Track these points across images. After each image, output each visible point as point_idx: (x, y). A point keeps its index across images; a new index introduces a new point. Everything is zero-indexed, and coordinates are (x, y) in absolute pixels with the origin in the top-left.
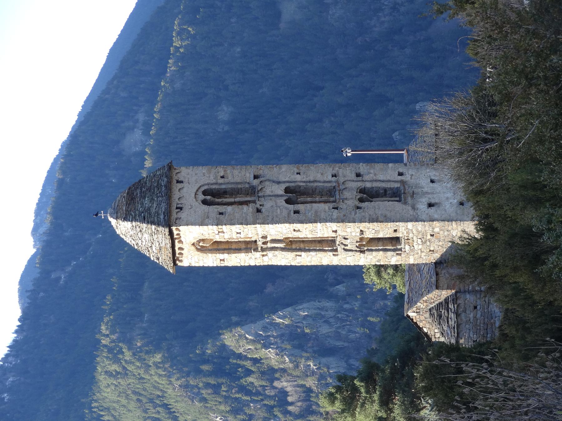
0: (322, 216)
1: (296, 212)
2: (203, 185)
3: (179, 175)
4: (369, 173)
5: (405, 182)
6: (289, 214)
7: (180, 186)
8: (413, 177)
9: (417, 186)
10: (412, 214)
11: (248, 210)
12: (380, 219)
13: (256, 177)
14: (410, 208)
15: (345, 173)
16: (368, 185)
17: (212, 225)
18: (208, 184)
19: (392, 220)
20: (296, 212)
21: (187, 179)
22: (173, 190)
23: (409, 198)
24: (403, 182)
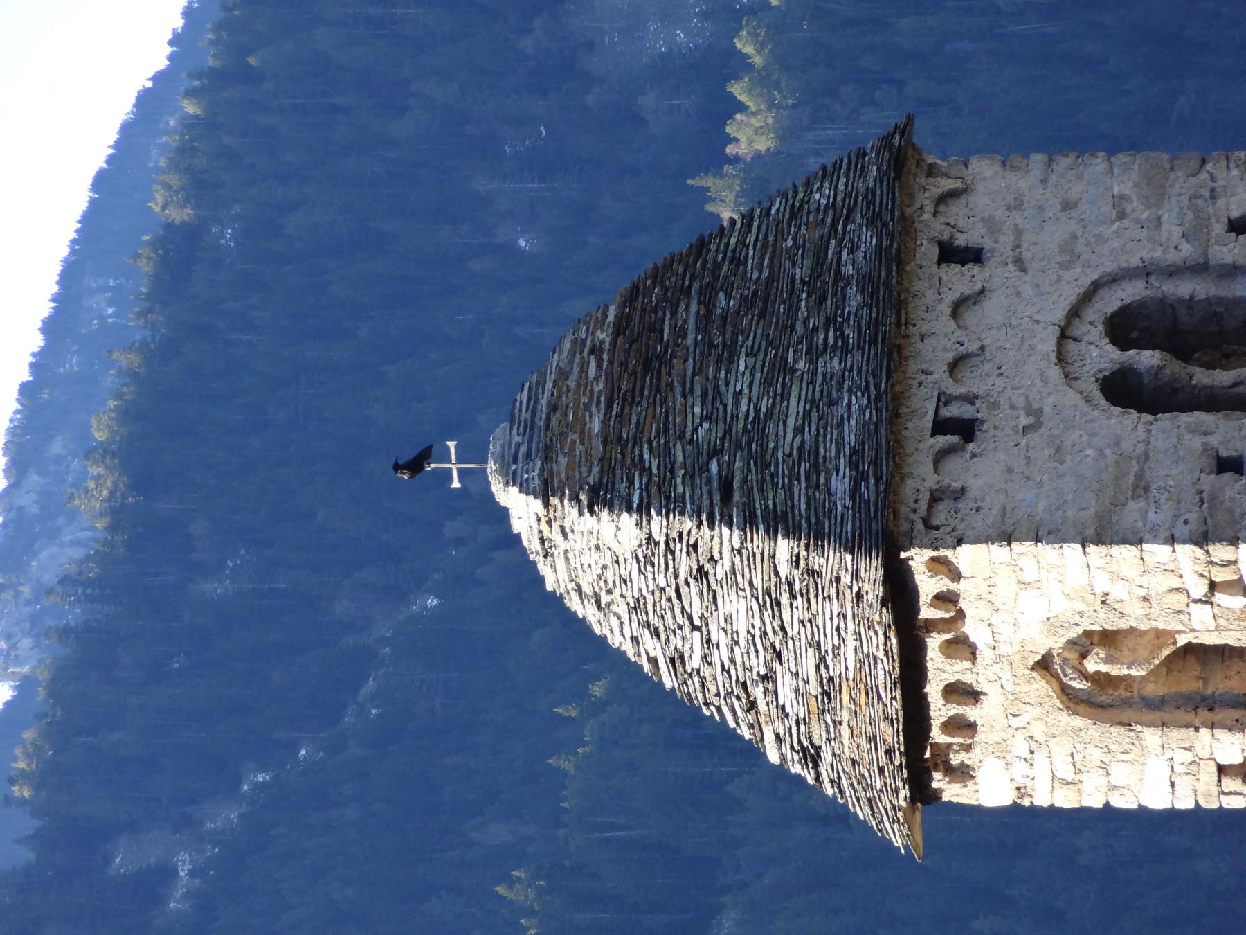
2: (1113, 280)
3: (956, 211)
17: (1172, 540)
18: (1146, 272)
21: (1007, 239)
22: (916, 309)
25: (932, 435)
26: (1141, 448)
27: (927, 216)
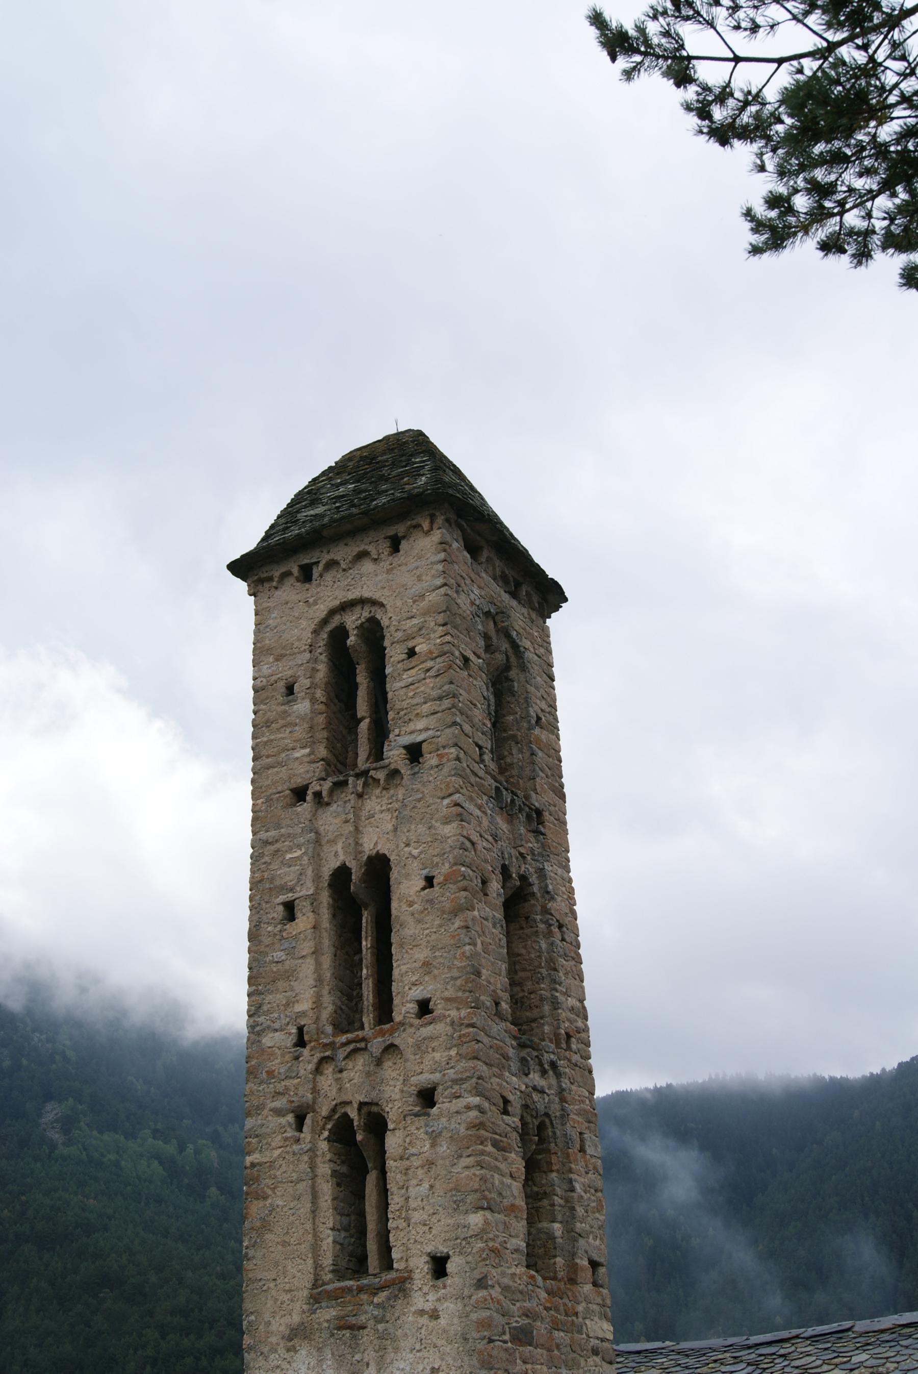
0: (270, 997)
1: (290, 910)
4: (434, 1138)
6: (284, 889)
7: (385, 547)
8: (424, 1320)
10: (274, 1327)
11: (303, 763)
13: (414, 752)
14: (296, 1319)
15: (435, 1044)
16: (392, 1142)
17: (255, 679)
19: (251, 1253)
20: (290, 910)
23: (334, 1313)
24: (402, 1286)
25: (299, 566)
26: (296, 651)
27: (409, 523)
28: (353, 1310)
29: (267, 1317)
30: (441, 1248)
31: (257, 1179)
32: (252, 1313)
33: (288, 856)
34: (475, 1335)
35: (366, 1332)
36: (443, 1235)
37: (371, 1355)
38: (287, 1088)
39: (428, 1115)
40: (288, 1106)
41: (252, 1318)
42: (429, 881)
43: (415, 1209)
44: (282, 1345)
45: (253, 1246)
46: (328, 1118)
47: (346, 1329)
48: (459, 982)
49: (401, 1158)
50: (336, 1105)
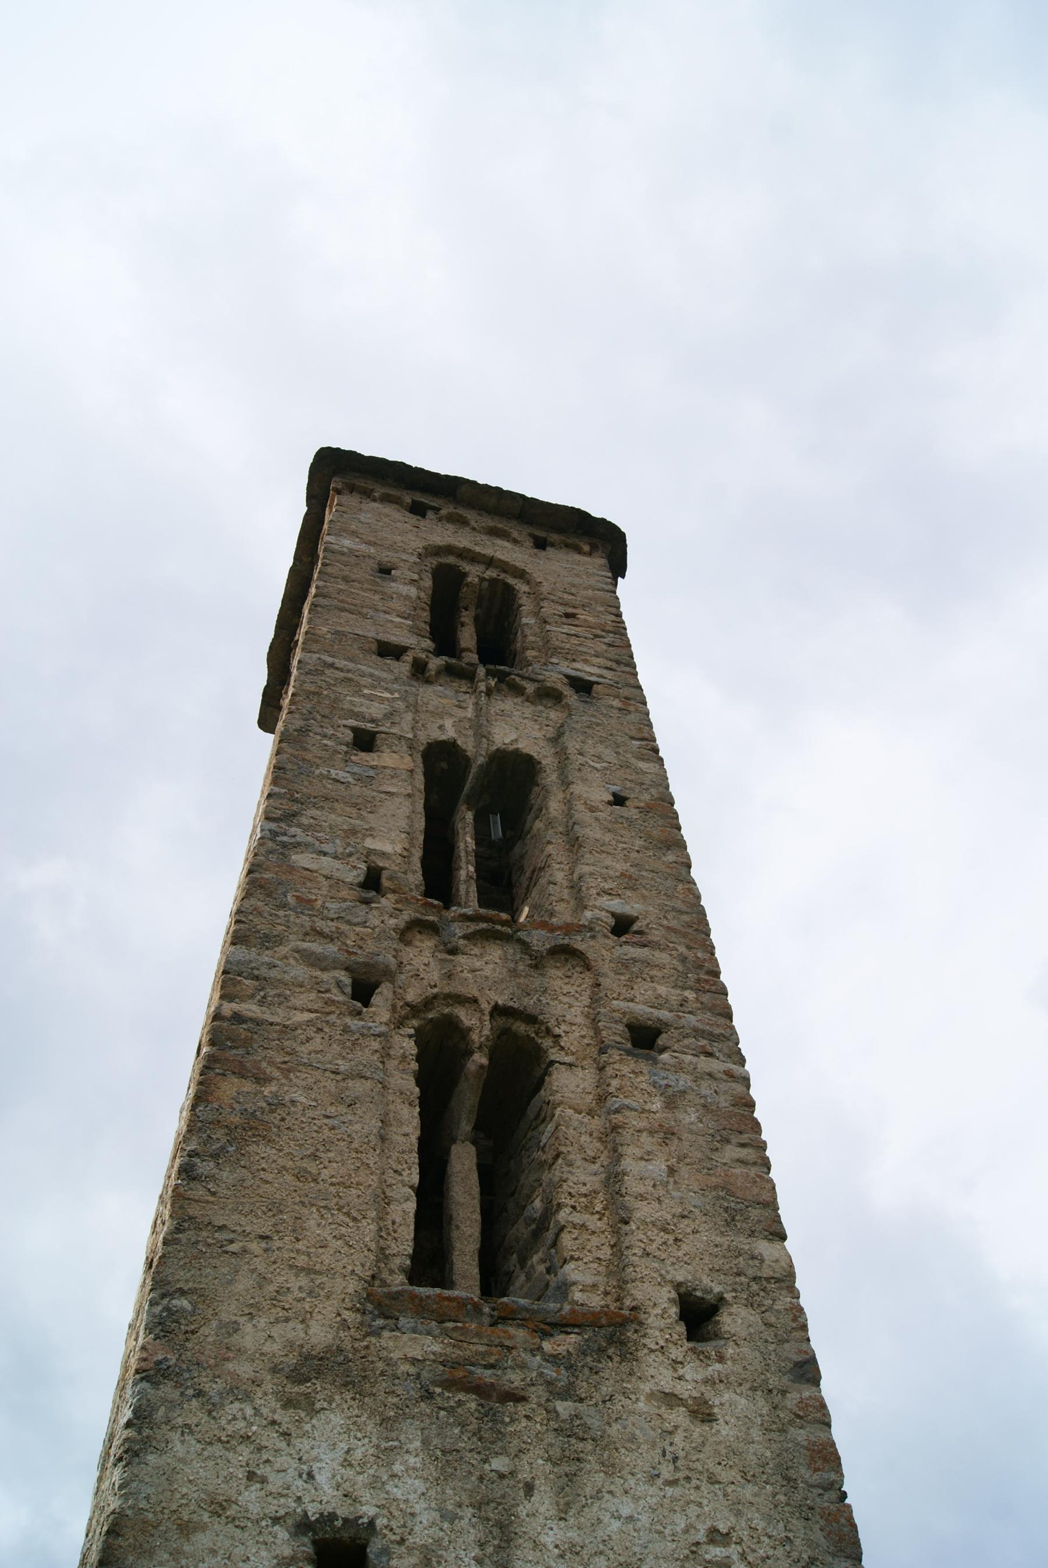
5: (627, 1353)
8: (678, 1416)
9: (577, 1448)
10: (249, 1337)
12: (229, 1088)
14: (320, 1334)
15: (654, 972)
16: (569, 1085)
19: (205, 1167)
24: (614, 1331)
28: (483, 1355)
29: (229, 1311)
30: (706, 1281)
31: (247, 1043)
32: (182, 1292)
33: (366, 691)
34: (805, 1472)
35: (522, 1409)
36: (707, 1259)
37: (535, 1465)
38: (341, 934)
39: (655, 1062)
40: (343, 957)
41: (184, 1303)
42: (619, 800)
43: (641, 1197)
44: (268, 1387)
45: (215, 1156)
46: (415, 1010)
47: (468, 1390)
48: (686, 918)
49: (591, 1113)
50: (435, 997)
